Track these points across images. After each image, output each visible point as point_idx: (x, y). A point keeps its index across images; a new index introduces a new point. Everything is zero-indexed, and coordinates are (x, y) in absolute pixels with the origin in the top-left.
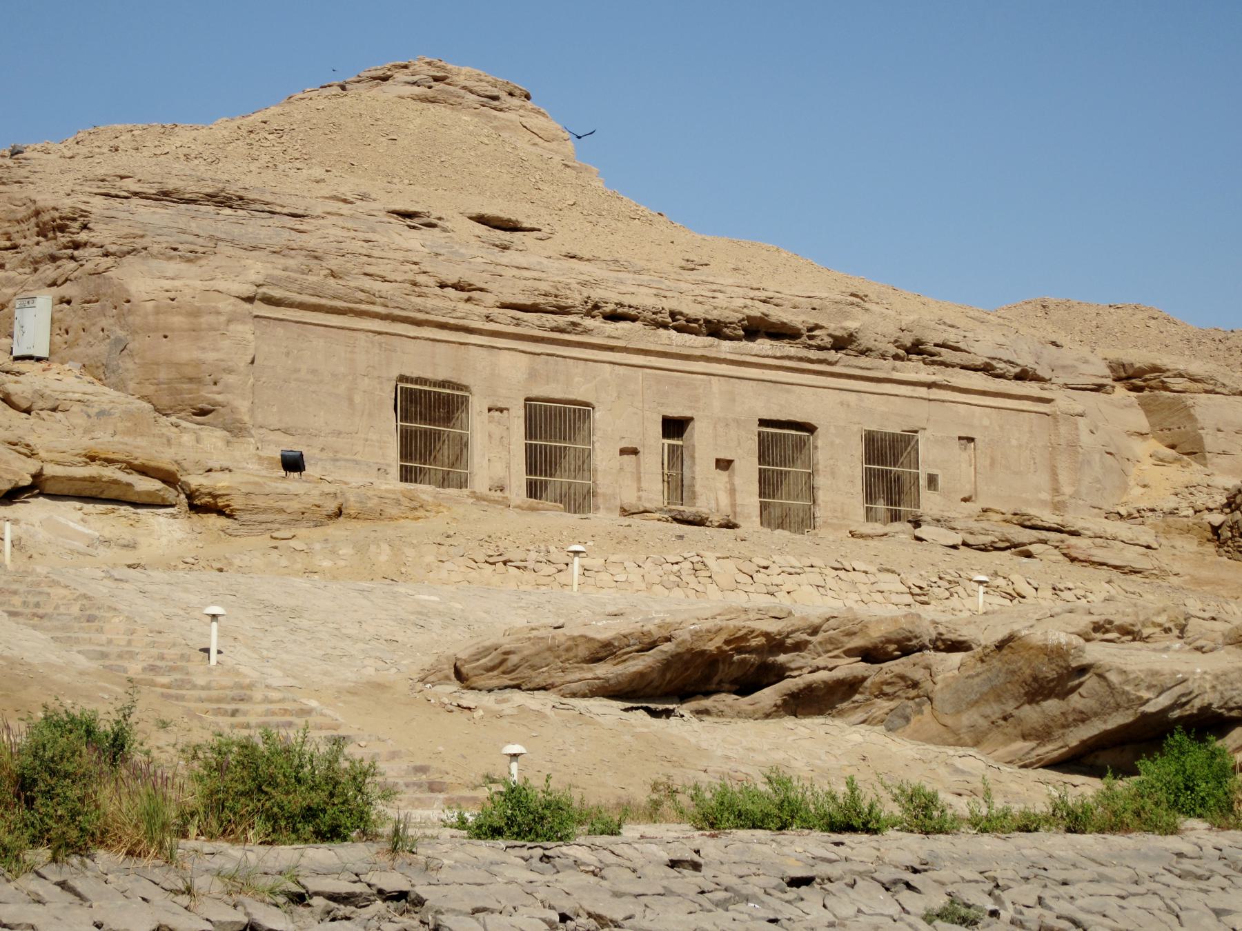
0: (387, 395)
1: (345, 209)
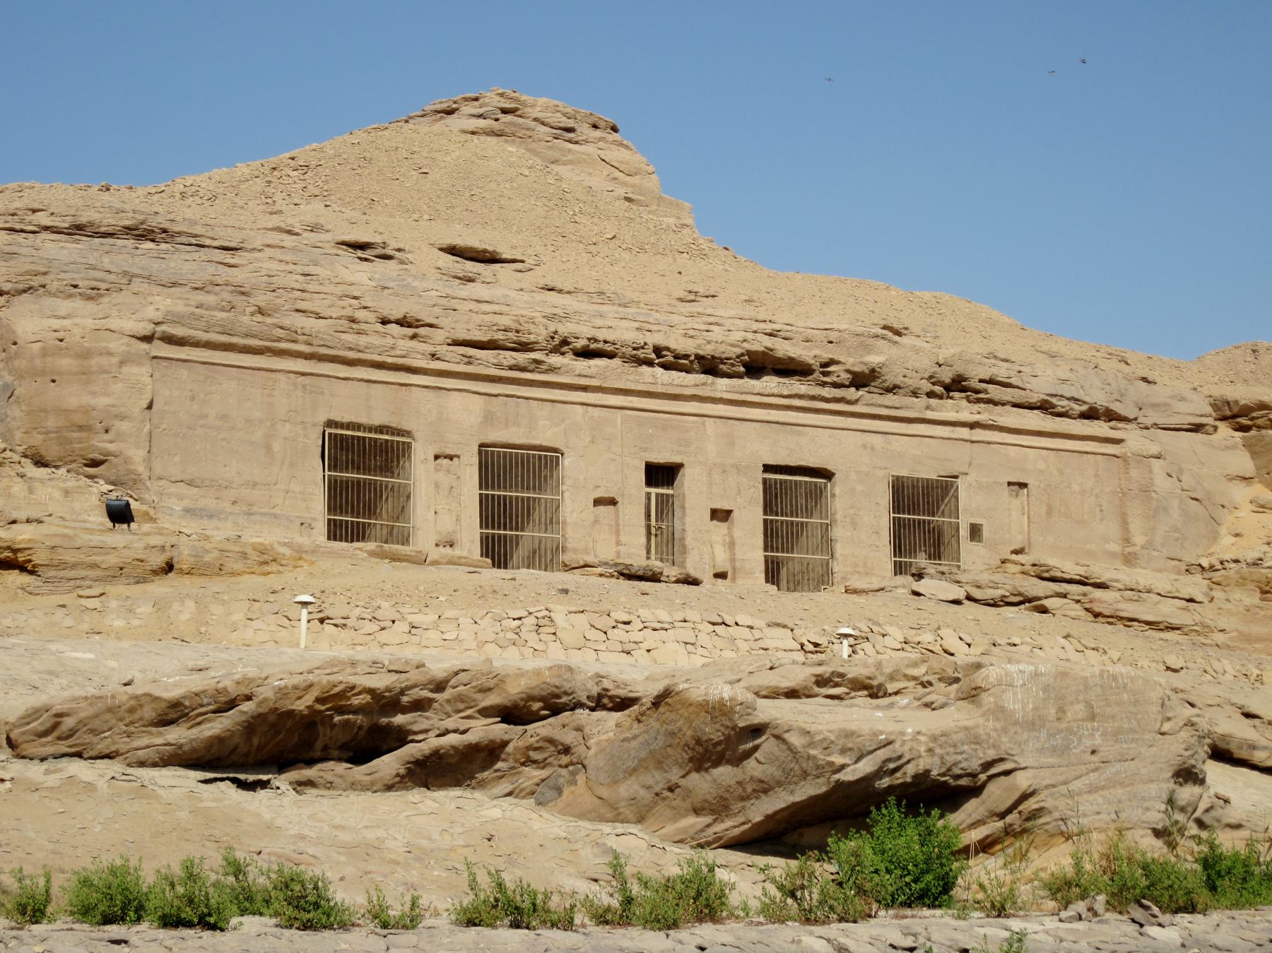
1: (288, 241)
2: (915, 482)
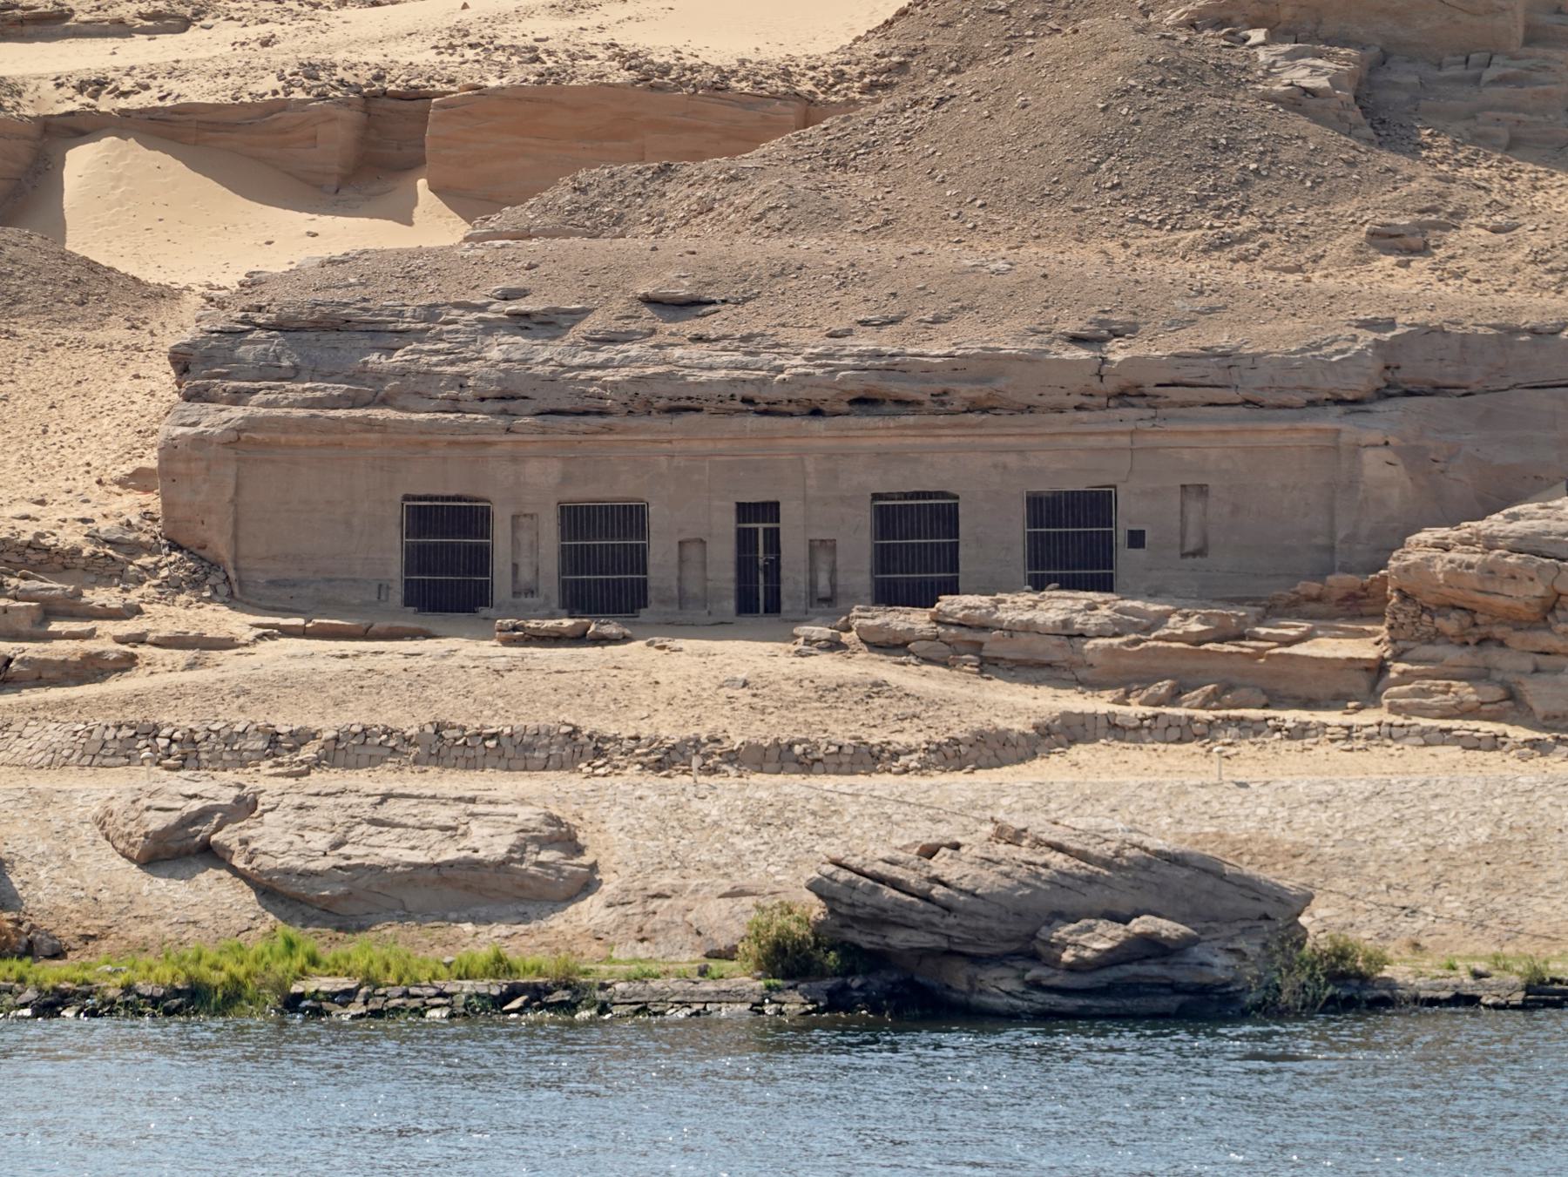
0: (393, 517)
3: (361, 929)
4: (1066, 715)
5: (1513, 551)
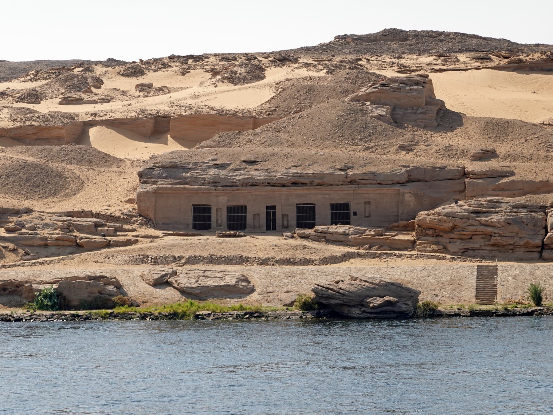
2: (337, 204)
3: (205, 300)
4: (348, 252)
5: (445, 216)
